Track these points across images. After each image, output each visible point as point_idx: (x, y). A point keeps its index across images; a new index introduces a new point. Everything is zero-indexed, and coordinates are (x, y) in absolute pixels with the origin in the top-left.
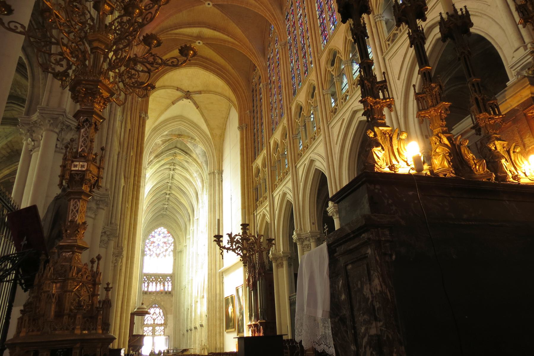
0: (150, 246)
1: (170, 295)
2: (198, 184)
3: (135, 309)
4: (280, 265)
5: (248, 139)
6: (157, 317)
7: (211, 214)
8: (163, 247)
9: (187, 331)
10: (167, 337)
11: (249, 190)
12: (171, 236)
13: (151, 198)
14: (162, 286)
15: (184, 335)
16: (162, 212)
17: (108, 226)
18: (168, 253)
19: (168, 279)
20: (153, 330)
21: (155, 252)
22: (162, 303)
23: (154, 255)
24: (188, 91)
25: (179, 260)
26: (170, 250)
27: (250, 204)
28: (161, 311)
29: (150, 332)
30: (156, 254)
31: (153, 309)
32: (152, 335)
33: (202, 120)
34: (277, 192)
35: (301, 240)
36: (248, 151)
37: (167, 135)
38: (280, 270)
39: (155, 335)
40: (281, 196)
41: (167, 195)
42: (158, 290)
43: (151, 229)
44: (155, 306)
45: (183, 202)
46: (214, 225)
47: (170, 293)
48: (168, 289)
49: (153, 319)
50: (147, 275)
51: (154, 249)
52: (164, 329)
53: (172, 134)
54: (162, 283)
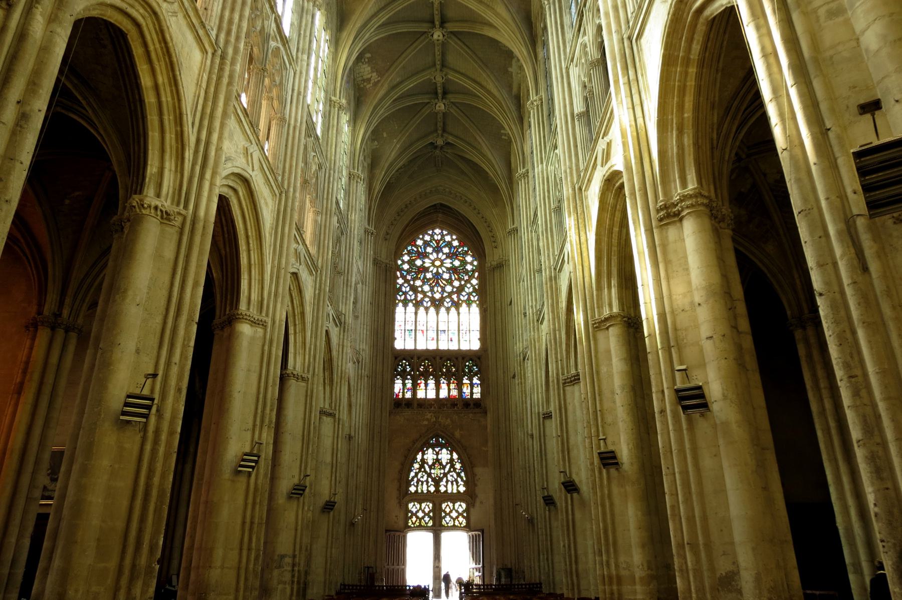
0: (414, 279)
1: (477, 410)
10: (477, 533)
14: (452, 386)
15: (531, 521)
21: (429, 294)
22: (457, 434)
23: (427, 303)
28: (455, 456)
29: (427, 519)
30: (433, 300)
31: (430, 450)
32: (434, 525)
41: (434, 27)
42: (443, 394)
43: (406, 207)
47: (477, 403)
48: (472, 393)
49: (433, 480)
51: (426, 288)
52: (466, 511)
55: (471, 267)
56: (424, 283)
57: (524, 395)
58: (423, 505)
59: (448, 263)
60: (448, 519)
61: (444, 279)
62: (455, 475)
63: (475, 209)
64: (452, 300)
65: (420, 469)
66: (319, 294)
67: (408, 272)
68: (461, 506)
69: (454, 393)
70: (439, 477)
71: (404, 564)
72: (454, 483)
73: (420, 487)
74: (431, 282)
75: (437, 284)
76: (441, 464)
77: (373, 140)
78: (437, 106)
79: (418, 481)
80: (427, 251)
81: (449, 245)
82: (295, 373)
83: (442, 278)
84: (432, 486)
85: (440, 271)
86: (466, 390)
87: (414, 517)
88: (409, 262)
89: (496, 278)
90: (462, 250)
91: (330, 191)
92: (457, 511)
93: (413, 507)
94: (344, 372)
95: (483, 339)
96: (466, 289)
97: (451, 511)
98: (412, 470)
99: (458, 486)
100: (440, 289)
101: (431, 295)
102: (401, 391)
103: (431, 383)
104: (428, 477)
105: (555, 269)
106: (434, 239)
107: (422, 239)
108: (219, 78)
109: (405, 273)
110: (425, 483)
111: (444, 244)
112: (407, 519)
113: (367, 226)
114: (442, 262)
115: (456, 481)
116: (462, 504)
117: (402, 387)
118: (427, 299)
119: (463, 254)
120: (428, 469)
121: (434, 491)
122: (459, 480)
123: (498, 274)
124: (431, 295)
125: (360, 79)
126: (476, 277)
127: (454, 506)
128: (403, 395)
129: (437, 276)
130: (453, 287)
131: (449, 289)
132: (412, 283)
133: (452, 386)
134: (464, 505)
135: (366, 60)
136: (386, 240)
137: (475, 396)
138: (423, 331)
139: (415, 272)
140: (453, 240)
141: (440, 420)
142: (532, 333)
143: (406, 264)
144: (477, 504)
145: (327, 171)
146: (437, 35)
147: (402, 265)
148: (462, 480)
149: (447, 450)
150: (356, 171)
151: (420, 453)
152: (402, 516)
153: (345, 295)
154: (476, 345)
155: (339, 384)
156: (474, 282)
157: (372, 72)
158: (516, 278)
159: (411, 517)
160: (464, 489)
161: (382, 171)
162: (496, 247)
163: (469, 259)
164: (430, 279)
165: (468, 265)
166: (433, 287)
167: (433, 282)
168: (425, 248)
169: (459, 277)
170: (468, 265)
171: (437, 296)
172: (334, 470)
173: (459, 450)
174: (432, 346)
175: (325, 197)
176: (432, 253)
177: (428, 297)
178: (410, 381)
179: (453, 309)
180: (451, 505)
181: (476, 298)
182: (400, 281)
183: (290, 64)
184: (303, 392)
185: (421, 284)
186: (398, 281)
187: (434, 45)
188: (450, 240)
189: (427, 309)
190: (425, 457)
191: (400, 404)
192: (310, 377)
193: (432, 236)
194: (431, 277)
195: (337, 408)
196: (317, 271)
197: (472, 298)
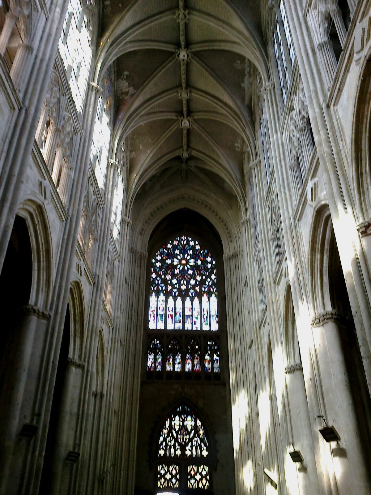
0: (165, 274)
8: (194, 277)
14: (196, 362)
18: (205, 288)
22: (201, 403)
28: (199, 423)
29: (174, 481)
30: (179, 290)
31: (177, 418)
42: (188, 367)
43: (158, 209)
44: (183, 408)
48: (212, 368)
51: (175, 281)
52: (209, 473)
56: (173, 278)
57: (261, 360)
59: (192, 262)
60: (193, 481)
63: (214, 211)
64: (195, 291)
66: (68, 239)
68: (204, 470)
69: (197, 367)
70: (185, 443)
72: (198, 448)
75: (183, 278)
76: (186, 430)
77: (131, 151)
78: (183, 122)
79: (167, 445)
81: (193, 248)
82: (36, 308)
84: (179, 450)
85: (186, 268)
86: (208, 365)
87: (163, 478)
88: (161, 261)
89: (232, 265)
91: (85, 154)
92: (201, 474)
93: (162, 469)
94: (95, 328)
96: (207, 283)
97: (195, 474)
98: (162, 436)
99: (201, 451)
100: (185, 282)
103: (179, 360)
105: (294, 218)
110: (172, 447)
112: (156, 480)
113: (124, 217)
114: (187, 262)
116: (205, 467)
118: (175, 290)
120: (175, 435)
122: (202, 444)
123: (234, 262)
124: (178, 287)
125: (120, 92)
126: (215, 273)
129: (184, 272)
130: (196, 281)
131: (193, 282)
132: (163, 277)
133: (196, 362)
134: (207, 468)
135: (125, 77)
136: (141, 234)
137: (215, 371)
138: (171, 316)
142: (270, 294)
143: (159, 263)
145: (83, 138)
146: (183, 55)
147: (155, 263)
148: (205, 445)
149: (192, 417)
151: (168, 420)
153: (99, 258)
154: (215, 327)
155: (89, 338)
156: (213, 277)
157: (130, 86)
158: (250, 259)
159: (160, 478)
162: (231, 241)
163: (209, 259)
167: (180, 276)
170: (208, 264)
171: (184, 287)
172: (80, 421)
174: (178, 326)
175: (80, 157)
176: (179, 255)
179: (196, 298)
180: (195, 468)
182: (154, 276)
183: (42, 8)
184: (43, 328)
186: (152, 276)
187: (180, 65)
189: (175, 299)
192: (52, 314)
193: (179, 242)
195: (87, 360)
196: (68, 218)
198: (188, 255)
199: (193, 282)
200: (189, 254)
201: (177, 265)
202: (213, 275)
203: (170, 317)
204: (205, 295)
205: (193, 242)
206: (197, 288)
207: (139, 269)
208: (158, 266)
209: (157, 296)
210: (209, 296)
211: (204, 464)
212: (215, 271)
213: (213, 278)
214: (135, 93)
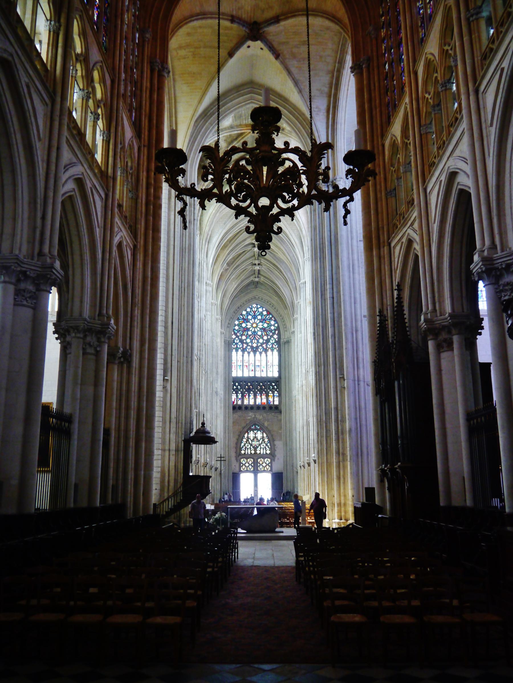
0: (242, 335)
1: (276, 411)
2: (300, 220)
3: (191, 433)
4: (445, 345)
5: (372, 87)
6: (260, 445)
7: (316, 263)
8: (262, 337)
9: (300, 467)
11: (379, 196)
12: (273, 318)
13: (228, 254)
14: (263, 397)
15: (297, 472)
16: (252, 278)
17: (32, 259)
19: (272, 386)
20: (254, 463)
21: (250, 344)
22: (266, 424)
23: (249, 349)
24: (255, 23)
25: (287, 356)
26: (272, 341)
27: (380, 226)
28: (265, 435)
29: (250, 467)
30: (252, 347)
31: (252, 432)
33: (290, 84)
34: (434, 179)
35: (493, 273)
36: (374, 113)
37: (231, 127)
38: (445, 355)
39: (257, 470)
40: (443, 183)
42: (258, 401)
43: (238, 308)
44: (255, 427)
45: (281, 257)
46: (323, 283)
47: (277, 407)
50: (236, 380)
51: (248, 341)
52: (271, 463)
53: (240, 125)
54: (264, 393)
55: (274, 327)
58: (249, 460)
59: (260, 325)
60: (261, 467)
61: (258, 335)
62: (265, 445)
63: (275, 308)
65: (246, 442)
67: (238, 331)
69: (264, 401)
71: (239, 489)
73: (246, 451)
74: (251, 337)
76: (257, 439)
79: (246, 448)
80: (249, 318)
81: (261, 314)
83: (257, 334)
85: (256, 330)
86: (271, 399)
88: (238, 325)
90: (269, 317)
92: (266, 463)
93: (243, 461)
95: (280, 372)
96: (271, 341)
97: (263, 463)
99: (266, 451)
100: (256, 341)
101: (251, 345)
102: (236, 400)
103: (252, 396)
104: (251, 446)
106: (252, 311)
107: (246, 310)
108: (200, 367)
109: (236, 332)
111: (258, 313)
112: (240, 467)
114: (257, 324)
115: (265, 448)
117: (236, 398)
118: (249, 347)
119: (269, 319)
120: (250, 442)
121: (254, 454)
122: (267, 447)
124: (251, 345)
127: (264, 460)
128: (237, 402)
130: (264, 340)
132: (240, 337)
136: (228, 327)
138: (247, 366)
139: (242, 331)
140: (263, 311)
141: (257, 416)
143: (237, 326)
144: (276, 459)
148: (268, 448)
149: (261, 432)
150: (218, 317)
151: (246, 434)
152: (238, 465)
154: (276, 375)
156: (276, 336)
159: (242, 466)
160: (269, 452)
161: (227, 299)
163: (273, 322)
164: (250, 335)
165: (272, 326)
166: (252, 340)
168: (247, 316)
169: (267, 334)
170: (272, 326)
173: (266, 432)
174: (252, 374)
176: (251, 320)
177: (250, 346)
178: (241, 395)
179: (263, 353)
180: (263, 460)
181: (276, 346)
185: (245, 338)
188: (262, 311)
189: (249, 353)
190: (249, 435)
191: (236, 408)
193: (251, 308)
194: (251, 334)
197: (274, 346)
198: (258, 320)
199: (261, 341)
200: (258, 318)
201: (250, 328)
202: (275, 335)
203: (246, 367)
204: (270, 350)
205: (261, 309)
206: (264, 346)
207: (228, 353)
208: (236, 329)
209: (237, 351)
210: (272, 350)
211: (267, 458)
212: (277, 332)
213: (275, 338)
214: (227, 269)
